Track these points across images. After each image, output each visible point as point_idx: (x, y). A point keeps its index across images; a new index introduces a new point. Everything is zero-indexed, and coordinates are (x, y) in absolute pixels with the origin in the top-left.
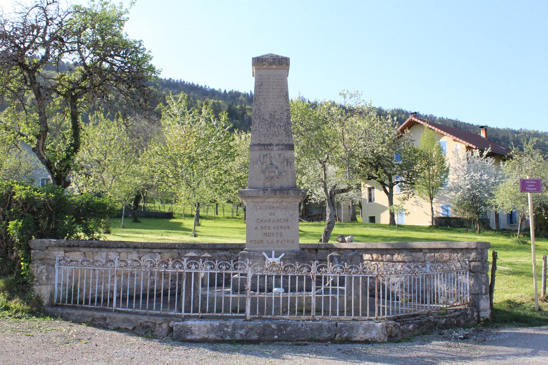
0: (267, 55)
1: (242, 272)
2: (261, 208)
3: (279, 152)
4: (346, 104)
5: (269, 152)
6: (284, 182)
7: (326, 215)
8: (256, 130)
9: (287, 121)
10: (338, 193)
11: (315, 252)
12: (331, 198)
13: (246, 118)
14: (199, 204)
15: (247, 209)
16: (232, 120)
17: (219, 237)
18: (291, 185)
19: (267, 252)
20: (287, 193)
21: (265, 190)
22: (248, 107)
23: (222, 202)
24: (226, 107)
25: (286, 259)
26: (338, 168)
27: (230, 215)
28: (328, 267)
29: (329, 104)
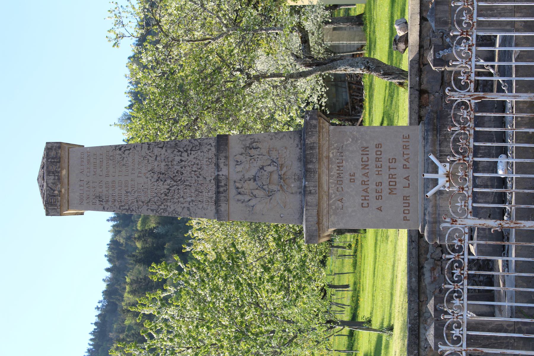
0: (41, 186)
1: (467, 236)
2: (341, 200)
3: (232, 163)
4: (135, 34)
5: (231, 184)
6: (290, 154)
7: (351, 75)
8: (188, 209)
9: (171, 147)
10: (310, 51)
11: (426, 96)
12: (318, 65)
13: (161, 230)
14: (329, 322)
15: (341, 226)
16: (164, 256)
17: (392, 283)
18: (297, 141)
19: (426, 188)
20: (312, 148)
21: (305, 192)
22: (139, 224)
23: (323, 277)
24: (140, 267)
25: (441, 151)
26: (260, 52)
27: (348, 262)
28: (457, 69)
29: (135, 66)
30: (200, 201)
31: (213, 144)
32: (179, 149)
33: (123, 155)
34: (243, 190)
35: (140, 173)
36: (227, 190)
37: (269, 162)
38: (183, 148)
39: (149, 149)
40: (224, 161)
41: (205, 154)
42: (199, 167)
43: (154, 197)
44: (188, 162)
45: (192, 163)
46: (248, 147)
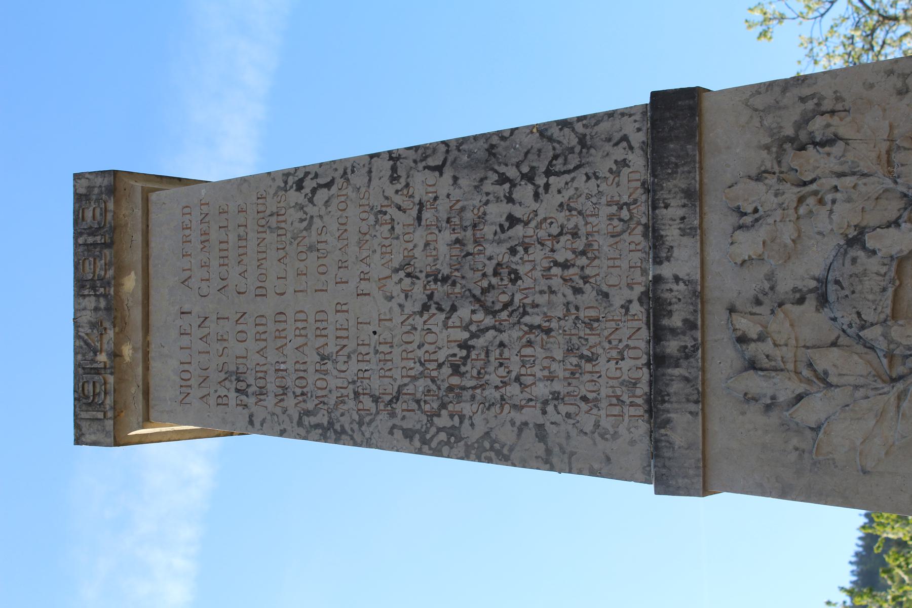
3: (718, 221)
5: (717, 318)
30: (584, 399)
31: (638, 139)
32: (502, 169)
33: (310, 209)
34: (766, 347)
35: (364, 277)
36: (695, 348)
37: (892, 208)
38: (518, 165)
39: (394, 179)
40: (681, 212)
41: (603, 187)
42: (580, 245)
43: (415, 378)
44: (538, 226)
45: (555, 230)
46: (791, 140)
